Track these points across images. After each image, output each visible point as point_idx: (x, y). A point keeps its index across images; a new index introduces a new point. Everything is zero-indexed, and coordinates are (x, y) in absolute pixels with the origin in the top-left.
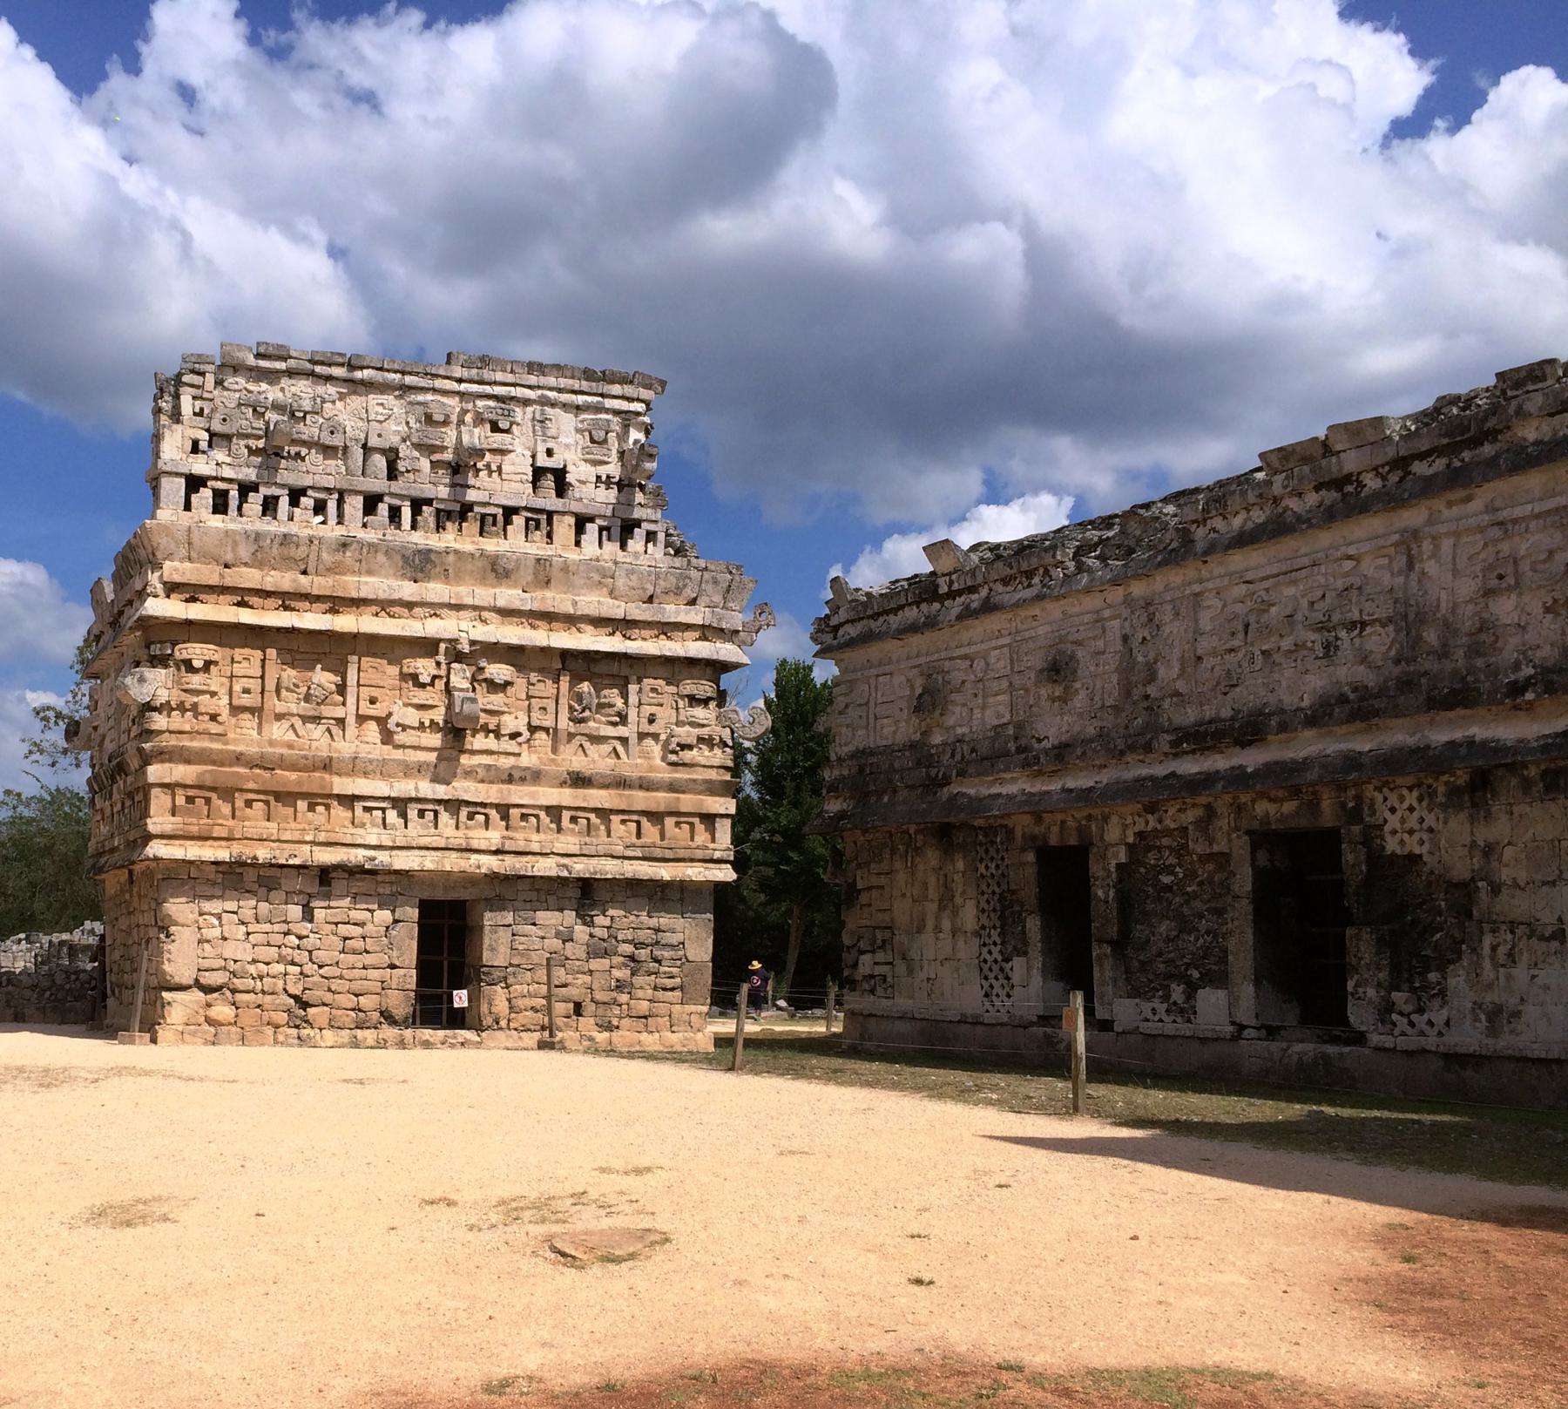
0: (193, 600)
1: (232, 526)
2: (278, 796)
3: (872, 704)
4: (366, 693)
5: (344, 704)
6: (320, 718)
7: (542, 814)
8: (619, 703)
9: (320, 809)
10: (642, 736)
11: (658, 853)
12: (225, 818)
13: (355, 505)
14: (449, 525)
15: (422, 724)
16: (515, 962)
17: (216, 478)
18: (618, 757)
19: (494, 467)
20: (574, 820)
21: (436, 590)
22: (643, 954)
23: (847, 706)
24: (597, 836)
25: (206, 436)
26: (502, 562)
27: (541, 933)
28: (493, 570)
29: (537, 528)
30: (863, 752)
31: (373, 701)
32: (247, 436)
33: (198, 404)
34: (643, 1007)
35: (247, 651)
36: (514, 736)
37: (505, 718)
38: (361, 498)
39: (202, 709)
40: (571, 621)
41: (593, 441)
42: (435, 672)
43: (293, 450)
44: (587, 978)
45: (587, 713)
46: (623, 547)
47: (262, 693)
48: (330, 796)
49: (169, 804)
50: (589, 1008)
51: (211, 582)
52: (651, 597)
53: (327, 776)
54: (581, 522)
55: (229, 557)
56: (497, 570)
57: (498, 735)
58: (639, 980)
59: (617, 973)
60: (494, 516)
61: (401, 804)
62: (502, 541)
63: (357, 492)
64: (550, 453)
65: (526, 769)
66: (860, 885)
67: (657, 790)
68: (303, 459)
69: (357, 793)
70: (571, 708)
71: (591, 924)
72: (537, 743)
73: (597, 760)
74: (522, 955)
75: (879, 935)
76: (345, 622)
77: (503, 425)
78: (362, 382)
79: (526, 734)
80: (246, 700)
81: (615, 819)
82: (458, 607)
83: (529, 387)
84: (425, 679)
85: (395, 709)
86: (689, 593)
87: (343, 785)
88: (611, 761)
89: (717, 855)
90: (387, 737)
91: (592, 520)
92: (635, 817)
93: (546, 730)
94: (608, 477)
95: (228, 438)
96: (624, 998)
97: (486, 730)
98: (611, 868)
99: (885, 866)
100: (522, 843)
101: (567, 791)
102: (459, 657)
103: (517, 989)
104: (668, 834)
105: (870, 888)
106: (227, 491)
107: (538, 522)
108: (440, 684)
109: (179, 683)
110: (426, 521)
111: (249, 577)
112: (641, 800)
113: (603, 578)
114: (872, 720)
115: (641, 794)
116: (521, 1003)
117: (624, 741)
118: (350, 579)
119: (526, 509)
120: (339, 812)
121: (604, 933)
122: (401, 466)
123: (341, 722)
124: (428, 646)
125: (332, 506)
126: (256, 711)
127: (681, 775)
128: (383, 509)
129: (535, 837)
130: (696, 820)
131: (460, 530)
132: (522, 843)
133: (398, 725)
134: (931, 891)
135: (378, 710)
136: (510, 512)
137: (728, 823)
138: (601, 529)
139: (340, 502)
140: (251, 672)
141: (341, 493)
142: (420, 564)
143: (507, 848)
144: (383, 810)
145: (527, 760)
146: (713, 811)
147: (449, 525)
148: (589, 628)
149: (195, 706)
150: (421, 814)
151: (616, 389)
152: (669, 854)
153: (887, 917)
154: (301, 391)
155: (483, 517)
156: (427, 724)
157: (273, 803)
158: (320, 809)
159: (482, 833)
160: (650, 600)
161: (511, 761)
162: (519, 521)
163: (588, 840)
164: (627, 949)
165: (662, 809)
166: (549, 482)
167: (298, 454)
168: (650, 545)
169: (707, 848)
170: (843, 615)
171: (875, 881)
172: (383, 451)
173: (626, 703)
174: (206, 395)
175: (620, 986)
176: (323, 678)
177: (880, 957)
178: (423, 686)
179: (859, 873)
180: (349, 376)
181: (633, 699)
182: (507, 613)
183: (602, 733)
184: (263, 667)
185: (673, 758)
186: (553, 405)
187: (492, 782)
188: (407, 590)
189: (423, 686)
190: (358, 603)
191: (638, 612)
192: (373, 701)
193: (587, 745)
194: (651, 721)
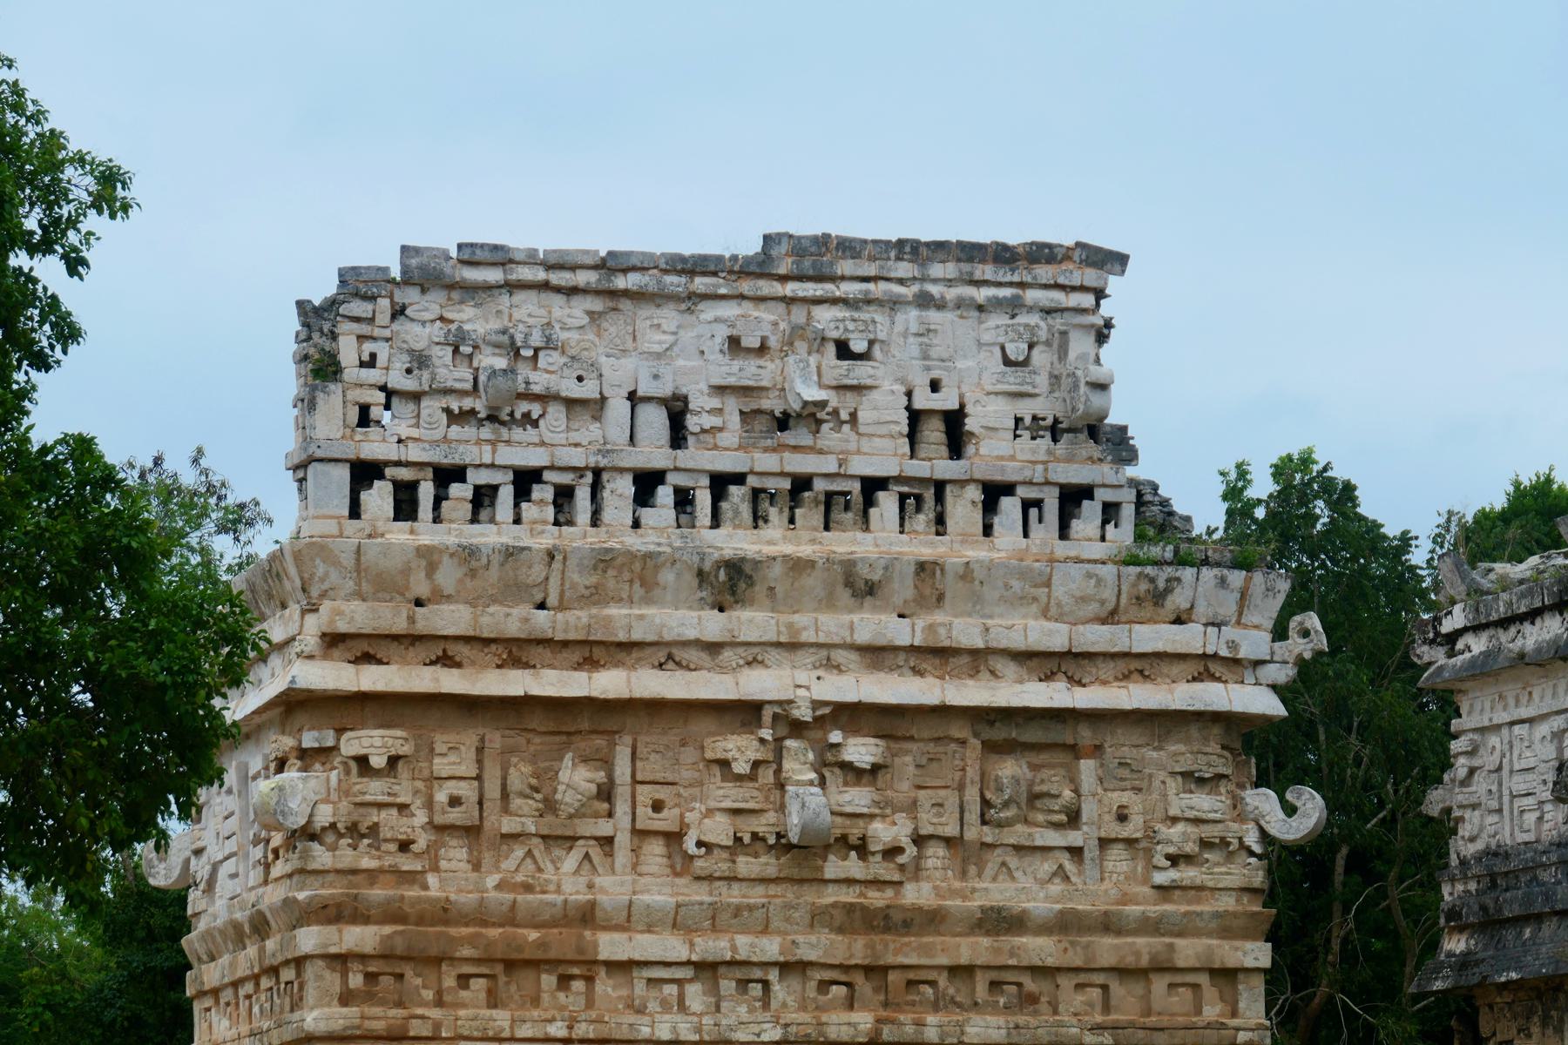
0: (368, 658)
1: (425, 540)
2: (511, 965)
3: (1505, 772)
4: (645, 794)
5: (610, 815)
6: (575, 839)
7: (943, 980)
9: (578, 985)
10: (1104, 843)
12: (425, 1004)
13: (621, 489)
14: (773, 512)
15: (738, 840)
17: (398, 464)
18: (1067, 878)
19: (844, 416)
20: (995, 985)
21: (753, 622)
23: (1472, 771)
24: (1036, 1013)
25: (381, 397)
26: (864, 571)
28: (849, 583)
29: (918, 509)
31: (657, 806)
32: (448, 392)
33: (368, 347)
35: (452, 737)
36: (892, 852)
38: (629, 478)
39: (385, 833)
40: (978, 659)
41: (1007, 362)
42: (759, 756)
43: (522, 407)
46: (1064, 532)
47: (480, 803)
48: (595, 962)
49: (337, 988)
51: (395, 630)
52: (1114, 612)
53: (587, 933)
54: (994, 493)
55: (421, 589)
56: (862, 587)
57: (862, 848)
61: (707, 969)
62: (859, 535)
63: (622, 470)
67: (1136, 932)
68: (535, 424)
69: (637, 957)
72: (930, 863)
73: (1030, 890)
76: (609, 683)
77: (858, 346)
78: (626, 293)
79: (911, 850)
80: (455, 816)
81: (1067, 982)
82: (793, 646)
83: (901, 281)
84: (741, 767)
85: (690, 817)
87: (611, 946)
88: (1056, 888)
90: (680, 863)
91: (1008, 489)
94: (1035, 418)
95: (416, 397)
97: (844, 844)
100: (910, 1029)
101: (985, 941)
102: (797, 728)
104: (1156, 1006)
106: (413, 486)
107: (919, 499)
108: (767, 776)
109: (347, 793)
110: (737, 513)
111: (450, 619)
112: (1107, 949)
113: (1034, 588)
115: (1109, 941)
117: (1076, 852)
118: (615, 611)
119: (900, 479)
120: (605, 987)
122: (692, 423)
123: (607, 842)
124: (746, 712)
125: (583, 495)
126: (471, 832)
128: (665, 494)
129: (931, 1019)
130: (1203, 979)
131: (792, 521)
132: (910, 1029)
133: (700, 844)
135: (666, 821)
136: (873, 486)
137: (1259, 984)
138: (1027, 505)
139: (596, 488)
140: (462, 770)
141: (597, 472)
142: (731, 582)
144: (679, 982)
145: (916, 894)
146: (1231, 963)
147: (773, 512)
148: (1009, 669)
149: (374, 829)
150: (743, 984)
151: (1044, 272)
154: (527, 311)
155: (830, 496)
156: (747, 839)
157: (502, 979)
158: (578, 985)
159: (846, 1017)
161: (890, 893)
162: (887, 503)
163: (1021, 1019)
165: (1144, 962)
166: (934, 433)
167: (527, 415)
168: (1110, 528)
169: (1223, 1026)
172: (663, 401)
173: (1076, 791)
174: (377, 332)
176: (576, 779)
178: (740, 778)
180: (605, 285)
182: (877, 655)
183: (1039, 842)
184: (479, 762)
185: (1160, 878)
186: (941, 305)
187: (854, 932)
188: (712, 625)
189: (740, 778)
190: (625, 650)
191: (1096, 637)
192: (657, 806)
194: (1122, 818)
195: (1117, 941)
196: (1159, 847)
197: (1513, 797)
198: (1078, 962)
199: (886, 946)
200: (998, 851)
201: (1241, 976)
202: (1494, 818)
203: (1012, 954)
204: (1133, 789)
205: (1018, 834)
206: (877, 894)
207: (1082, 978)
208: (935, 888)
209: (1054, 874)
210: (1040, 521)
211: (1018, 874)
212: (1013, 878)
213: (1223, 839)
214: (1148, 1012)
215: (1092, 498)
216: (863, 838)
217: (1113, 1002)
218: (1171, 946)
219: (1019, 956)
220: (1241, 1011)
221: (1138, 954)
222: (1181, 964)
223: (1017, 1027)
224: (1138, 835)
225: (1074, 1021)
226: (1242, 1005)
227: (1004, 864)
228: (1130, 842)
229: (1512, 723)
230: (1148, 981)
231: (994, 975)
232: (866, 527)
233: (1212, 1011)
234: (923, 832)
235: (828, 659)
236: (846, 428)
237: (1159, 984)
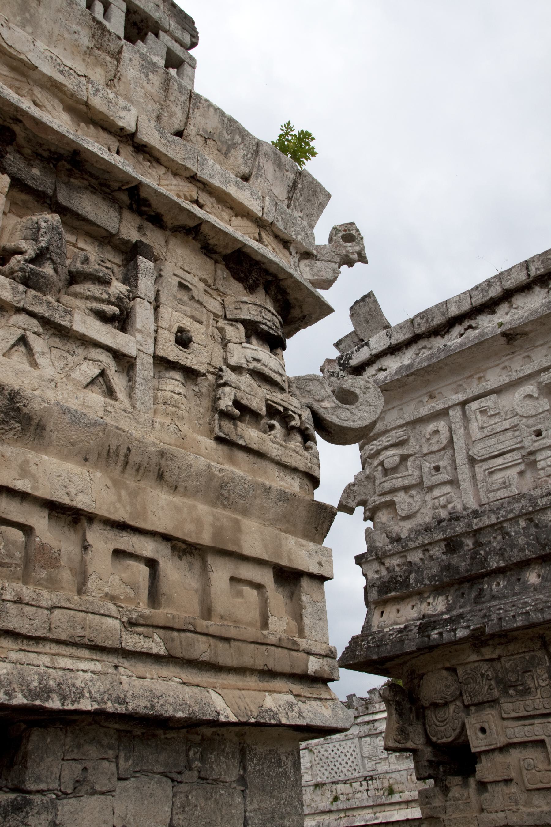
3: (459, 444)
8: (118, 287)
11: (202, 649)
18: (110, 392)
23: (404, 458)
24: (52, 584)
30: (454, 518)
66: (477, 743)
81: (101, 542)
88: (96, 398)
92: (147, 547)
99: (538, 702)
105: (505, 748)
114: (464, 472)
117: (125, 362)
127: (240, 470)
152: (226, 655)
169: (294, 648)
170: (378, 342)
171: (519, 732)
179: (472, 723)
181: (146, 285)
193: (38, 344)
194: (183, 340)
195: (177, 500)
196: (227, 389)
197: (472, 461)
198: (121, 514)
201: (305, 583)
202: (447, 489)
203: (24, 472)
204: (192, 317)
209: (93, 382)
211: (40, 360)
212: (34, 364)
213: (286, 409)
214: (207, 612)
217: (164, 587)
218: (237, 522)
219: (35, 479)
220: (307, 629)
221: (199, 522)
222: (247, 551)
223: (19, 601)
224: (202, 369)
225: (113, 610)
226: (307, 621)
227: (23, 340)
229: (463, 404)
230: (205, 569)
233: (280, 624)
237: (220, 573)
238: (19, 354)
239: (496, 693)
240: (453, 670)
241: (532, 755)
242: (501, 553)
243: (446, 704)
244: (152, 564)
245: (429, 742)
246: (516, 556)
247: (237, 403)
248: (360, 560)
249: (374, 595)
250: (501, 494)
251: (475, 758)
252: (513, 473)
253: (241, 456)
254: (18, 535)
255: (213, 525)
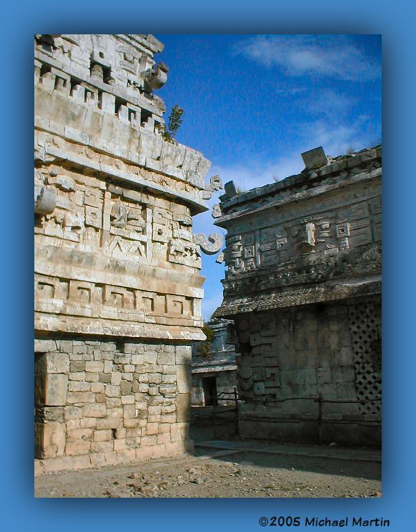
8: (141, 219)
16: (70, 401)
22: (154, 391)
27: (89, 379)
34: (154, 428)
36: (75, 228)
37: (69, 215)
41: (125, 59)
44: (120, 410)
45: (123, 221)
50: (121, 433)
58: (152, 409)
59: (141, 406)
60: (65, 81)
64: (101, 55)
65: (83, 254)
70: (112, 218)
71: (122, 370)
72: (89, 237)
74: (76, 396)
75: (269, 371)
79: (83, 228)
86: (179, 161)
88: (137, 257)
89: (195, 324)
91: (125, 103)
92: (150, 295)
93: (97, 230)
96: (143, 423)
98: (137, 331)
103: (73, 423)
107: (92, 93)
116: (77, 434)
117: (144, 243)
121: (129, 377)
134: (310, 345)
136: (75, 82)
143: (68, 311)
148: (124, 166)
153: (274, 362)
155: (57, 78)
160: (158, 159)
161: (73, 246)
162: (80, 88)
163: (123, 310)
164: (144, 387)
171: (265, 341)
173: (145, 219)
175: (141, 414)
177: (270, 384)
179: (252, 337)
181: (149, 218)
185: (172, 259)
199: (71, 270)
200: (116, 237)
201: (195, 300)
203: (121, 281)
205: (124, 232)
206: (68, 246)
207: (145, 294)
208: (92, 248)
210: (135, 118)
215: (151, 117)
216: (64, 220)
227: (118, 243)
228: (162, 243)
229: (260, 229)
231: (113, 289)
232: (71, 94)
234: (87, 223)
235: (53, 141)
236: (66, 55)
237: (170, 299)
238: (117, 248)
239: (259, 329)
240: (248, 320)
241: (268, 348)
242: (265, 284)
243: (245, 331)
244: (152, 299)
245: (239, 342)
246: (269, 286)
247: (176, 251)
248: (222, 281)
249: (225, 294)
250: (269, 264)
251: (252, 348)
252: (272, 257)
253: (176, 265)
254: (121, 296)
255: (168, 287)
